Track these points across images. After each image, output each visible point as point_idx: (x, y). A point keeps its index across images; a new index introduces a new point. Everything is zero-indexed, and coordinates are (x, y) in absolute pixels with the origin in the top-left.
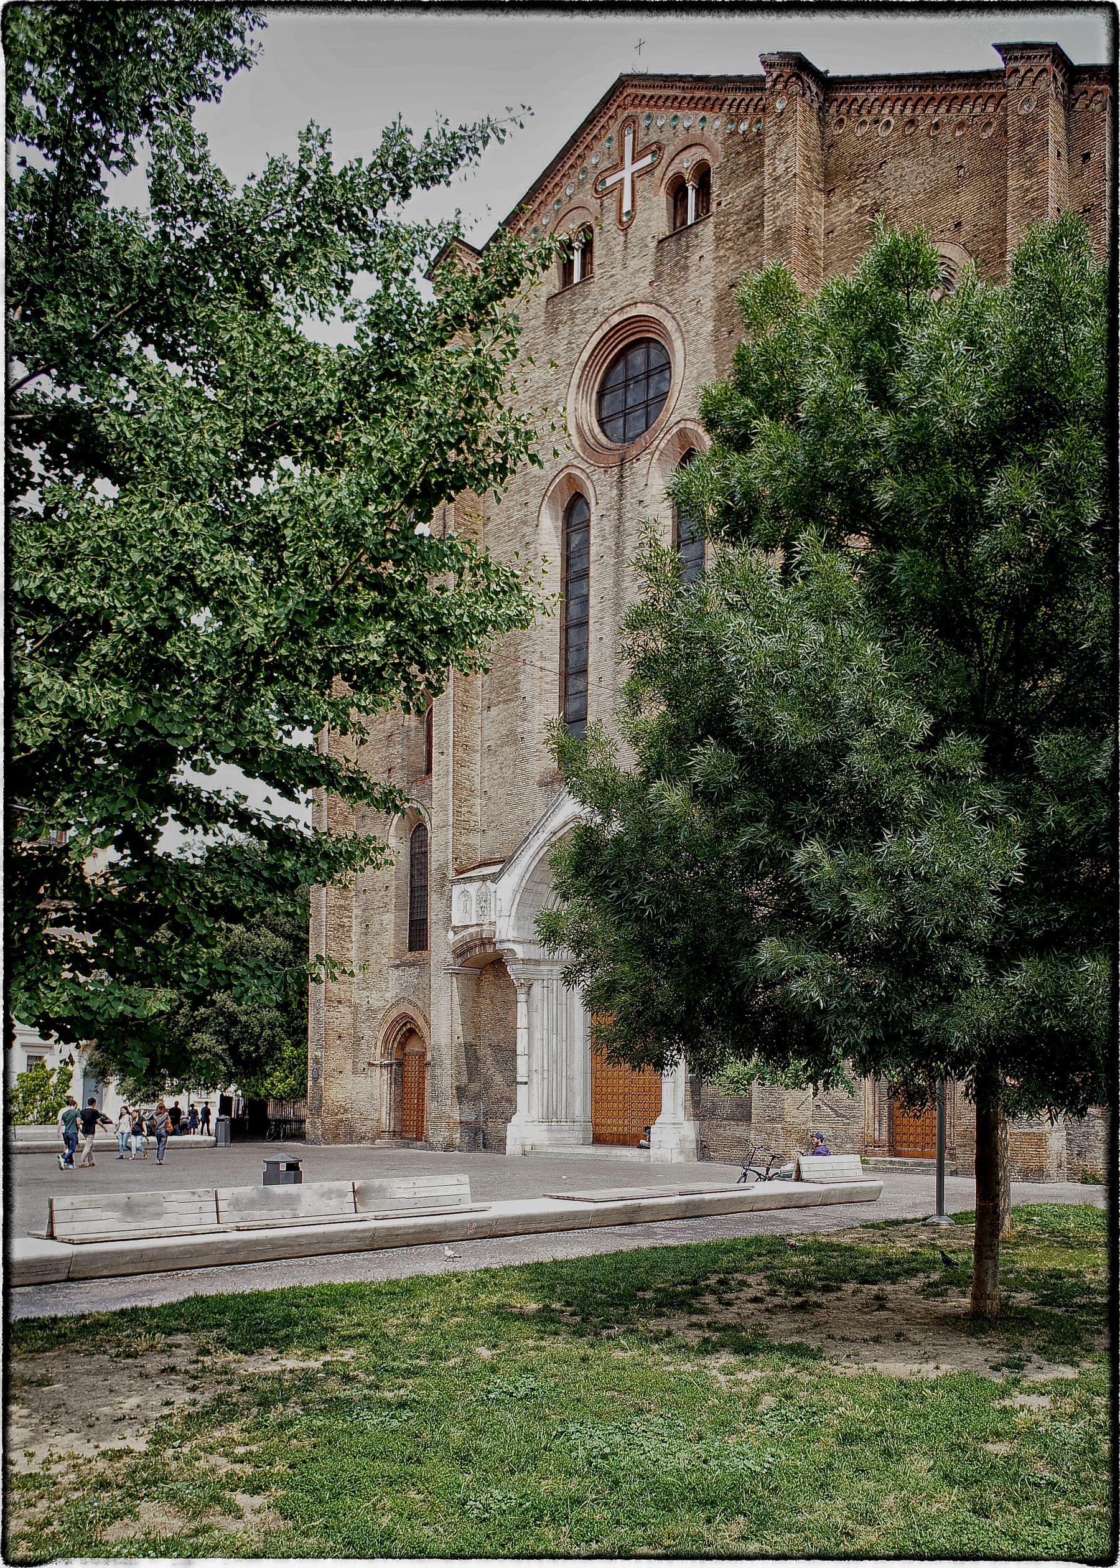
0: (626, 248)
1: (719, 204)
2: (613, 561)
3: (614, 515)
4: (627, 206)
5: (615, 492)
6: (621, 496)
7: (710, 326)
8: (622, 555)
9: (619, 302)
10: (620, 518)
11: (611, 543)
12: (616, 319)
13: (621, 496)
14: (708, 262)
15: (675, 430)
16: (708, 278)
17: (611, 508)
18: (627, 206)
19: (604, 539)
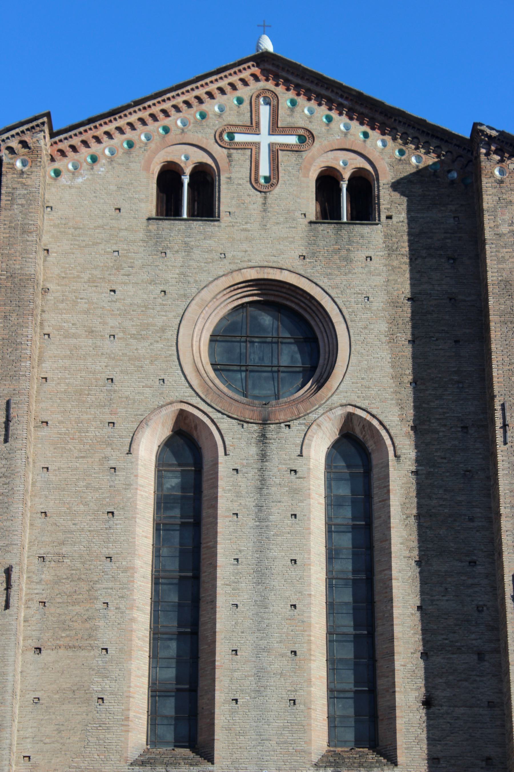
0: (265, 210)
1: (389, 217)
2: (252, 523)
3: (252, 473)
4: (264, 170)
5: (253, 450)
6: (263, 457)
7: (384, 327)
8: (266, 520)
9: (258, 259)
10: (263, 480)
11: (250, 502)
12: (253, 274)
13: (263, 457)
14: (378, 263)
15: (340, 412)
16: (379, 280)
17: (248, 465)
18: (264, 170)
19: (238, 495)
